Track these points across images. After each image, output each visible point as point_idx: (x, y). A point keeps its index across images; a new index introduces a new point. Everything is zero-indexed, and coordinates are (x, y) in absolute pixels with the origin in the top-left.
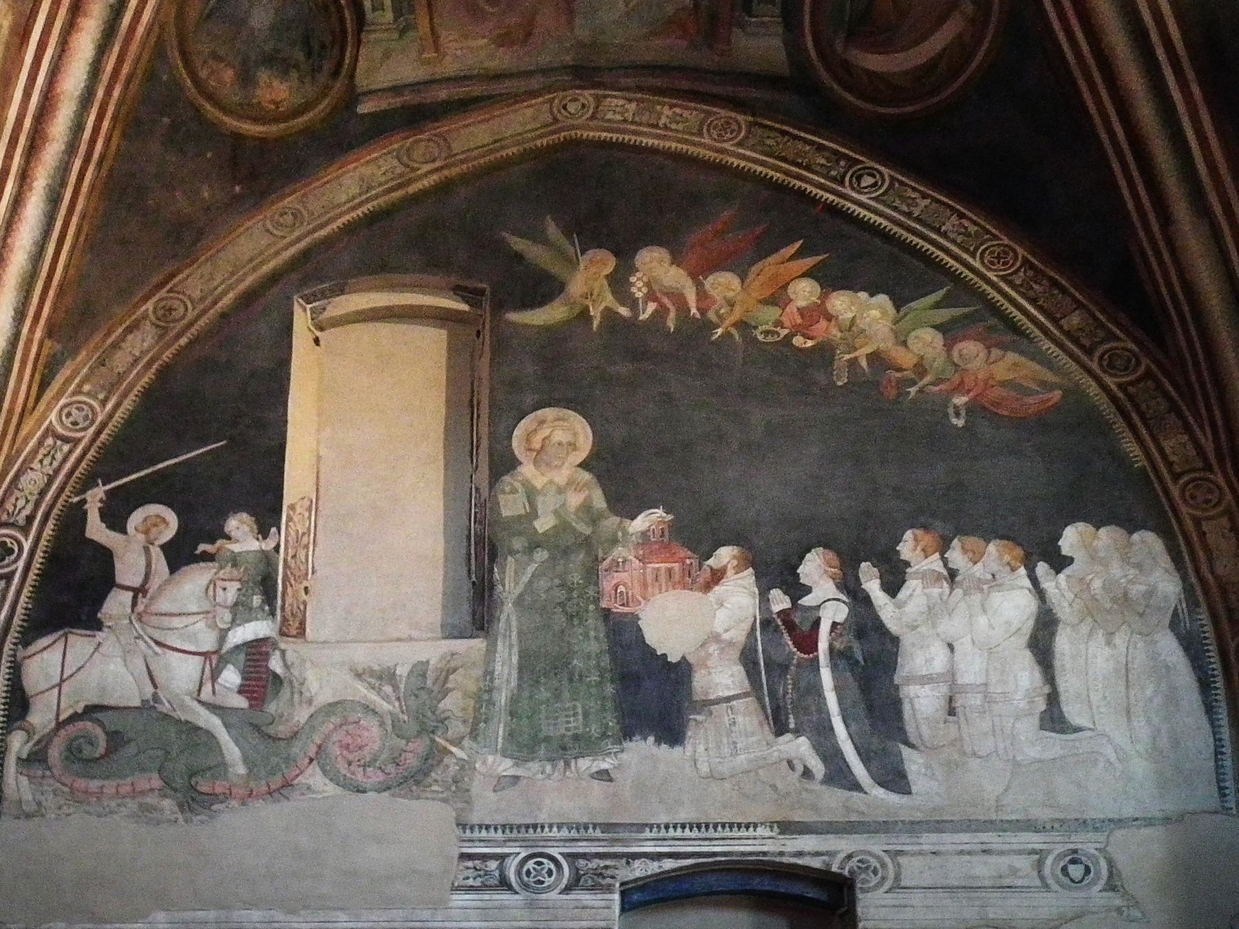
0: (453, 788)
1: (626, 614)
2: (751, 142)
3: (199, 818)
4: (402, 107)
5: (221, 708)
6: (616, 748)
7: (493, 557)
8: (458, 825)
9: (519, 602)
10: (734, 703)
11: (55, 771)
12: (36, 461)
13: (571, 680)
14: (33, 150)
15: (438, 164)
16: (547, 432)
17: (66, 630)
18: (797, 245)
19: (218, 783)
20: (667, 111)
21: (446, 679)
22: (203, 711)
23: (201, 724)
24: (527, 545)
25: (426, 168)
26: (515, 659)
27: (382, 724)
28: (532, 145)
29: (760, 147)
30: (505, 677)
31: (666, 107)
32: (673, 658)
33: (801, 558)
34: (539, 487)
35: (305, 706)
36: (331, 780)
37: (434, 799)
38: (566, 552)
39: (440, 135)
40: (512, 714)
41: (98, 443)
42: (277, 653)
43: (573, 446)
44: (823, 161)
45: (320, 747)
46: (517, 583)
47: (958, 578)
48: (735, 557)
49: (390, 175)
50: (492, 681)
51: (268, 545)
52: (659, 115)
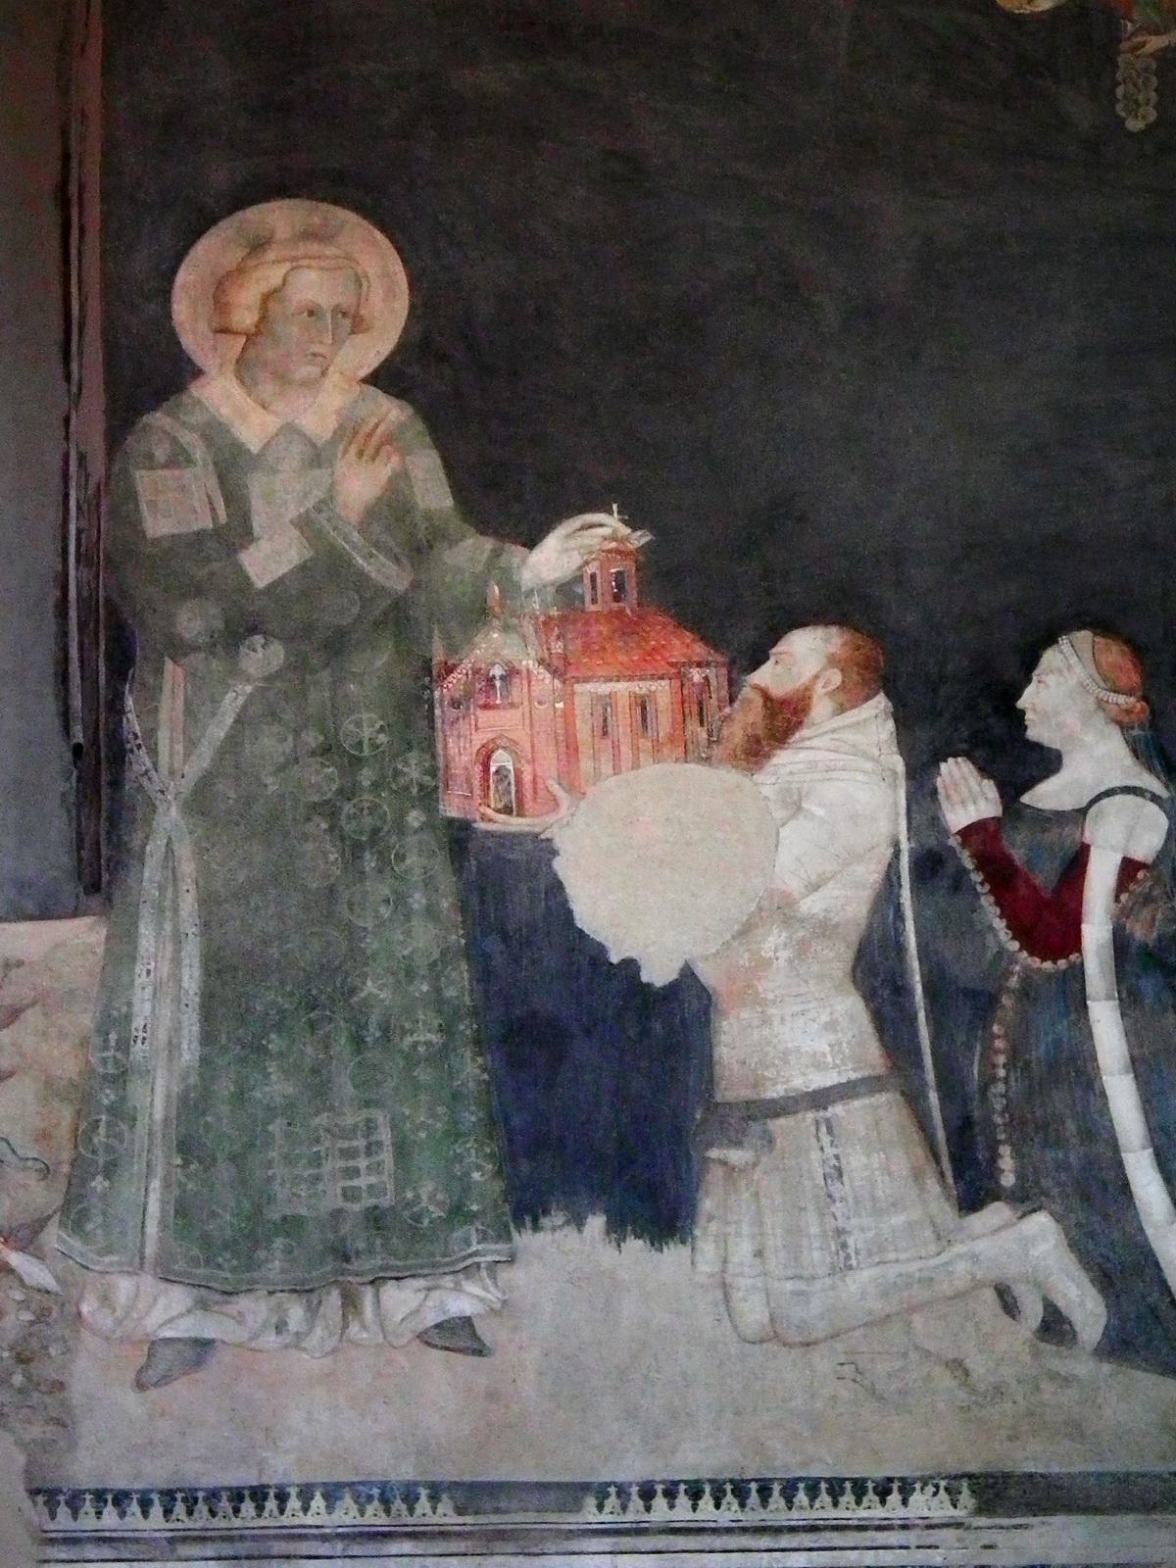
0: (18, 1379)
1: (516, 838)
6: (493, 1251)
7: (122, 662)
8: (34, 1493)
9: (200, 802)
10: (837, 1110)
13: (358, 1042)
16: (274, 276)
24: (219, 624)
26: (191, 979)
30: (162, 1035)
32: (658, 973)
33: (1029, 664)
34: (254, 447)
38: (337, 645)
40: (186, 1147)
43: (356, 322)
46: (191, 744)
48: (832, 661)
50: (124, 1045)
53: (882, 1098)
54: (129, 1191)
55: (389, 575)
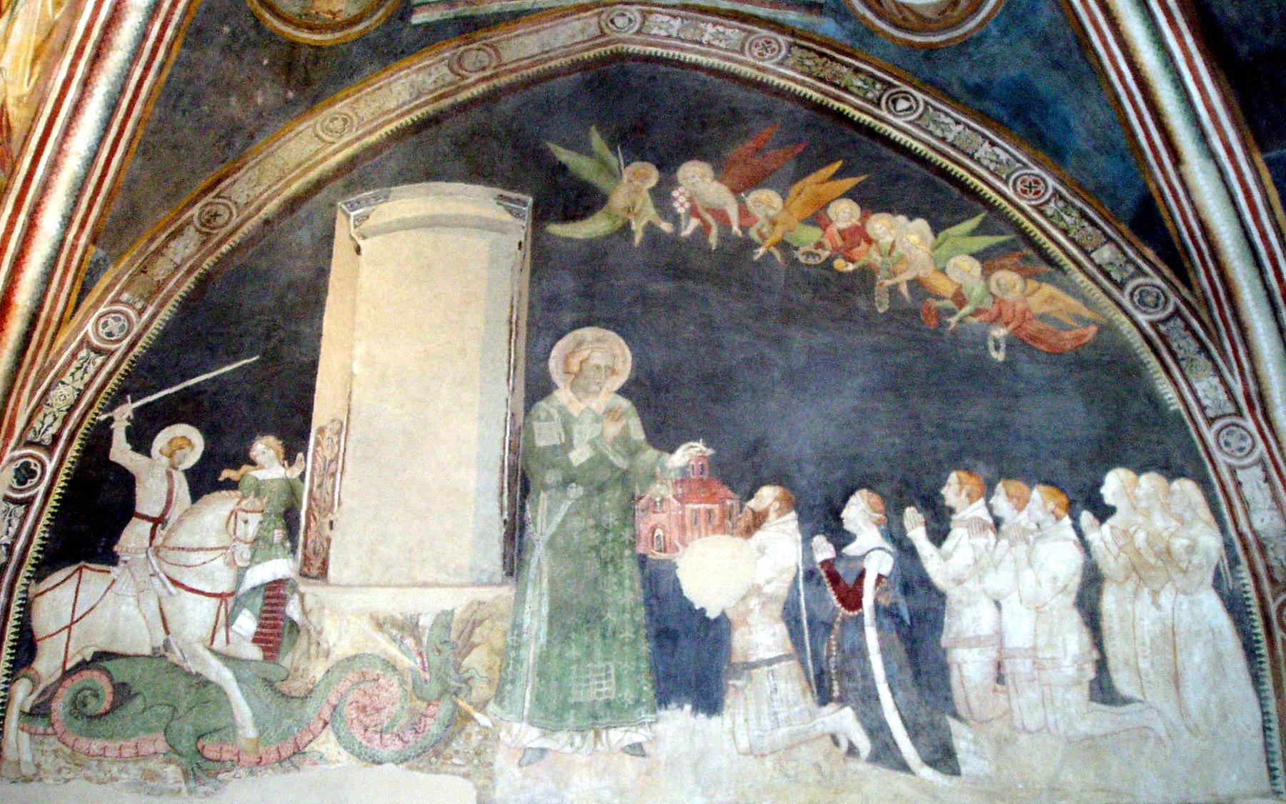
0: (476, 761)
1: (663, 561)
2: (790, 62)
3: (205, 788)
4: (456, 18)
5: (234, 659)
6: (649, 718)
7: (526, 491)
9: (551, 544)
10: (775, 666)
11: (56, 726)
12: (68, 373)
13: (604, 636)
14: (97, 57)
15: (488, 73)
16: (585, 354)
17: (82, 563)
18: (838, 165)
19: (225, 748)
20: (710, 29)
21: (471, 632)
22: (215, 662)
23: (213, 677)
24: (560, 479)
25: (474, 77)
26: (545, 610)
27: (402, 683)
28: (579, 56)
29: (799, 66)
30: (533, 632)
31: (710, 25)
32: (712, 614)
33: (845, 500)
34: (576, 415)
35: (322, 659)
36: (345, 748)
37: (453, 774)
38: (601, 489)
39: (491, 46)
40: (541, 674)
41: (131, 356)
42: (296, 597)
43: (612, 371)
44: (860, 84)
45: (335, 707)
46: (549, 522)
47: (1003, 527)
48: (776, 499)
49: (440, 83)
50: (519, 635)
51: (294, 472)
52: (703, 32)
53: (791, 662)
54: (518, 691)
55: (621, 462)
